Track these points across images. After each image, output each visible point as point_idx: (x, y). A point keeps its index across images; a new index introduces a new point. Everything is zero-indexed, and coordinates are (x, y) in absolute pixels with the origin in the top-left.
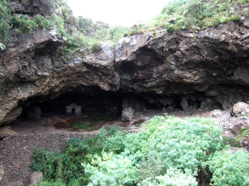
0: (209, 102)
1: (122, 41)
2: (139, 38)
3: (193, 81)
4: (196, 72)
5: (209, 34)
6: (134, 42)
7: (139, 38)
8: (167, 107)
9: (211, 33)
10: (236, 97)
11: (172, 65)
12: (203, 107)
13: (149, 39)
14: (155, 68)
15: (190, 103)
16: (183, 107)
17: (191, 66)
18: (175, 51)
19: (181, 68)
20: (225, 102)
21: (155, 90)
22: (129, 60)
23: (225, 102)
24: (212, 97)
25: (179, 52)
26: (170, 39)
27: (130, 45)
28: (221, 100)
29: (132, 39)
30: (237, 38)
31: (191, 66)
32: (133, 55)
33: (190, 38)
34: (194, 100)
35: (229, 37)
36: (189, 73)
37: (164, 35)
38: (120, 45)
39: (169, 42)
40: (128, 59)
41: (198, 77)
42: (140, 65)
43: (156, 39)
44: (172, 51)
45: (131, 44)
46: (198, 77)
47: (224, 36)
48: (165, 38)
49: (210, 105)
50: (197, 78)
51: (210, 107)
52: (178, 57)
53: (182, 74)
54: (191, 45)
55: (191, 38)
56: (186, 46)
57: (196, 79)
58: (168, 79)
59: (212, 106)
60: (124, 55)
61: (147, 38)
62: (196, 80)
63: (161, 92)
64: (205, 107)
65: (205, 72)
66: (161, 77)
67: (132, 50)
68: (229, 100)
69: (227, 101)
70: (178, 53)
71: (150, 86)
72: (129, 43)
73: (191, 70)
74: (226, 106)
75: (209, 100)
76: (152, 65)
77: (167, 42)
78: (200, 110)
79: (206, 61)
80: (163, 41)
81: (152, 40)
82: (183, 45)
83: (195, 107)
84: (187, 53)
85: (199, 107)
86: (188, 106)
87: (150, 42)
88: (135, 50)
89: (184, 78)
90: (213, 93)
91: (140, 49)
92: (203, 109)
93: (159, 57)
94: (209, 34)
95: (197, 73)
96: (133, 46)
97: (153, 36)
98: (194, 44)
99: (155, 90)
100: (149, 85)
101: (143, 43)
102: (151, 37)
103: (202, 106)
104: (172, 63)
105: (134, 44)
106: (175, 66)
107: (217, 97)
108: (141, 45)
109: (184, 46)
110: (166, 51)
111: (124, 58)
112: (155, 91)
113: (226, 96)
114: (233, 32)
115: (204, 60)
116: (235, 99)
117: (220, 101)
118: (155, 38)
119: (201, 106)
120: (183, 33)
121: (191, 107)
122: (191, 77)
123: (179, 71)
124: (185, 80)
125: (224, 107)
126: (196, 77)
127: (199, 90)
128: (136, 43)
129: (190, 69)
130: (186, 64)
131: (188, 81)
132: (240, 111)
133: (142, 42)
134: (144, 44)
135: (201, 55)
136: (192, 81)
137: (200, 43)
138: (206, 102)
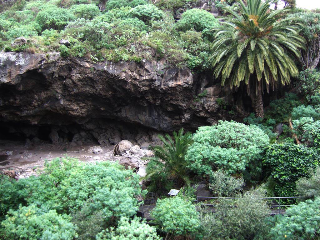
0: (83, 135)
1: (5, 58)
2: (28, 58)
3: (79, 114)
4: (84, 104)
5: (108, 68)
6: (22, 62)
7: (28, 58)
8: (31, 138)
9: (111, 68)
10: (114, 132)
11: (58, 93)
12: (75, 140)
13: (41, 62)
14: (37, 95)
15: (62, 135)
16: (52, 139)
17: (80, 98)
18: (65, 79)
19: (68, 98)
20: (102, 137)
21: (30, 119)
22: (13, 83)
23: (102, 137)
24: (88, 131)
25: (70, 80)
26: (63, 65)
27: (16, 65)
28: (97, 134)
29: (18, 57)
30: (136, 79)
31: (80, 98)
32: (18, 78)
33: (85, 68)
34: (67, 132)
35: (129, 76)
36: (76, 105)
37: (58, 60)
38: (2, 62)
39: (62, 68)
40: (11, 82)
41: (85, 110)
42: (21, 89)
43: (49, 63)
44: (61, 78)
45: (17, 64)
46: (85, 110)
47: (124, 74)
48: (57, 63)
49: (83, 139)
50: (84, 111)
51: (83, 141)
52: (68, 86)
53: (69, 105)
54: (86, 75)
55: (87, 67)
56: (80, 76)
57: (83, 112)
58: (50, 109)
59: (85, 140)
60: (6, 76)
61: (39, 60)
62: (82, 114)
63: (36, 123)
64: (78, 140)
65: (93, 105)
66: (42, 106)
67: (19, 71)
68: (107, 135)
69: (104, 135)
70: (68, 82)
71: (25, 114)
72: (14, 63)
73: (79, 102)
74: (103, 141)
75: (83, 134)
76: (34, 90)
77: (59, 67)
78: (73, 144)
79: (99, 96)
80: (55, 66)
81: (45, 64)
82: (76, 74)
83: (66, 140)
84: (79, 84)
85: (70, 140)
86: (58, 139)
87: (41, 66)
88: (22, 73)
89: (70, 110)
90: (90, 126)
91: (29, 72)
92: (76, 143)
93: (46, 83)
94: (108, 68)
95: (84, 106)
96: (20, 67)
97: (46, 59)
98: (90, 75)
99: (30, 119)
100: (25, 113)
101: (33, 65)
102: (44, 60)
103: (74, 140)
104: (59, 91)
105: (21, 64)
106: (61, 94)
107: (93, 131)
108: (32, 66)
109: (77, 75)
110: (55, 77)
111: (6, 81)
112: (30, 120)
113: (103, 131)
114: (133, 72)
115: (96, 94)
116: (113, 134)
117: (96, 135)
118: (49, 61)
119: (73, 139)
120: (78, 61)
121: (62, 139)
122: (77, 109)
123: (65, 102)
124: (70, 112)
125: (101, 141)
126: (83, 109)
127: (78, 123)
128: (24, 63)
129: (78, 100)
130: (76, 95)
131: (75, 114)
132: (125, 150)
133: (32, 63)
134: (35, 66)
135: (94, 87)
136: (78, 114)
137: (96, 75)
138: (80, 135)
